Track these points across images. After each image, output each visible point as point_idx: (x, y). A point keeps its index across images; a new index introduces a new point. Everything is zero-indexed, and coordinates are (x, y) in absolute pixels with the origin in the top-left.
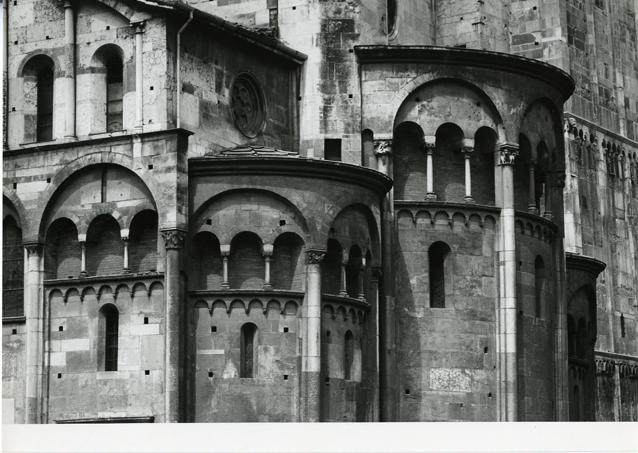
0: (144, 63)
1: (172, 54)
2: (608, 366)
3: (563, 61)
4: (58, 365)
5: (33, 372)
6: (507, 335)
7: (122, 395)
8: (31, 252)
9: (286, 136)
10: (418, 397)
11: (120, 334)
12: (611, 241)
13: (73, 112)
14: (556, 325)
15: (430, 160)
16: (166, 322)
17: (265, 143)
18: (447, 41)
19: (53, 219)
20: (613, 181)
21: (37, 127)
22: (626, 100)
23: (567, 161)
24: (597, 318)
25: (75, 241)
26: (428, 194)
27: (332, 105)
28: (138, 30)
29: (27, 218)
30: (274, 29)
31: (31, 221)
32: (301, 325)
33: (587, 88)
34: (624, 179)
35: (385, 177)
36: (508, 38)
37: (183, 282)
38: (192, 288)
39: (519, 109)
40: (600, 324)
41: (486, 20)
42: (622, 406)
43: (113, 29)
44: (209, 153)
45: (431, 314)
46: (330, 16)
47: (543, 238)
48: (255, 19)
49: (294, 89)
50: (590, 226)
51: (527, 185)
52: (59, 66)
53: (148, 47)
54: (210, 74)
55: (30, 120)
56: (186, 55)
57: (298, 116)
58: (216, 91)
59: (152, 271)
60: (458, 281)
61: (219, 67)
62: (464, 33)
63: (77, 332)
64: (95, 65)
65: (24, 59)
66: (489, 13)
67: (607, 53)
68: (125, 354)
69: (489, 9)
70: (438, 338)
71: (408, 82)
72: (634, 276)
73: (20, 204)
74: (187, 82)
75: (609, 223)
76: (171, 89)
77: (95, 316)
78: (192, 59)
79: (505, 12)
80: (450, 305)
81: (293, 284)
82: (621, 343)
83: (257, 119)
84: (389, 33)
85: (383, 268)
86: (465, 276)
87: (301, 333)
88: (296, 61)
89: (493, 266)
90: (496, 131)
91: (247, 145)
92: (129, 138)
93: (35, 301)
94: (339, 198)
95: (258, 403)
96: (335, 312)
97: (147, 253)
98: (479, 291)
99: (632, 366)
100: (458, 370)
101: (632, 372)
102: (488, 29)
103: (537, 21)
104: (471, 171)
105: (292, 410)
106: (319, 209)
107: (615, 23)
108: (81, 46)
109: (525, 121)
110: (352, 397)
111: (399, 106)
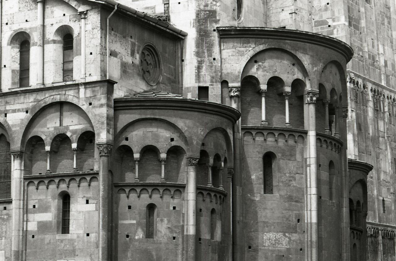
0: (86, 38)
1: (104, 32)
2: (375, 231)
3: (346, 37)
4: (32, 229)
5: (17, 234)
6: (312, 212)
7: (72, 249)
8: (16, 157)
9: (174, 84)
10: (256, 251)
11: (71, 210)
12: (376, 152)
13: (42, 68)
14: (342, 205)
15: (263, 100)
16: (100, 203)
17: (161, 89)
18: (274, 25)
19: (30, 137)
20: (377, 114)
21: (20, 78)
22: (386, 62)
23: (349, 101)
24: (368, 200)
25: (44, 151)
26: (262, 121)
27: (203, 65)
28: (83, 16)
29: (13, 136)
30: (167, 16)
31: (16, 138)
32: (183, 205)
33: (361, 54)
34: (384, 112)
35: (236, 111)
36: (312, 22)
37: (110, 177)
38: (116, 181)
39: (319, 67)
40: (369, 204)
41: (298, 11)
42: (384, 257)
43: (67, 16)
44: (127, 95)
45: (265, 198)
46: (201, 8)
47: (334, 150)
48: (155, 10)
49: (180, 55)
50: (363, 142)
51: (324, 116)
52: (33, 39)
53: (89, 27)
54: (127, 45)
55: (15, 73)
56: (113, 32)
57: (182, 72)
58: (131, 55)
59: (91, 170)
60: (281, 177)
61: (133, 40)
62: (285, 19)
63: (45, 209)
64: (56, 38)
65: (12, 34)
66: (300, 6)
67: (373, 32)
68: (74, 223)
69: (299, 4)
70: (269, 213)
71: (251, 49)
72: (391, 174)
73: (9, 127)
74: (113, 49)
75: (375, 140)
76: (103, 54)
77: (55, 199)
78: (116, 35)
79: (310, 6)
80: (276, 192)
81: (179, 179)
82: (383, 217)
83: (157, 74)
84: (238, 19)
85: (234, 169)
86: (286, 173)
87: (183, 210)
88: (181, 36)
89: (302, 167)
90: (305, 82)
91: (150, 90)
92: (77, 85)
93: (18, 189)
94: (207, 124)
95: (157, 255)
96: (205, 197)
97: (88, 159)
98: (294, 183)
99: (390, 231)
100: (281, 234)
101: (390, 235)
102: (299, 16)
103: (329, 11)
104: (289, 107)
105: (178, 259)
106: (195, 131)
107: (378, 13)
108: (47, 26)
109: (323, 75)
110: (215, 250)
111: (244, 66)
